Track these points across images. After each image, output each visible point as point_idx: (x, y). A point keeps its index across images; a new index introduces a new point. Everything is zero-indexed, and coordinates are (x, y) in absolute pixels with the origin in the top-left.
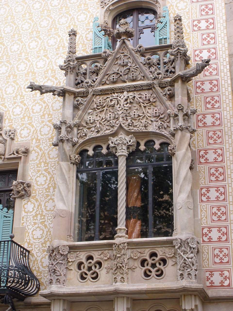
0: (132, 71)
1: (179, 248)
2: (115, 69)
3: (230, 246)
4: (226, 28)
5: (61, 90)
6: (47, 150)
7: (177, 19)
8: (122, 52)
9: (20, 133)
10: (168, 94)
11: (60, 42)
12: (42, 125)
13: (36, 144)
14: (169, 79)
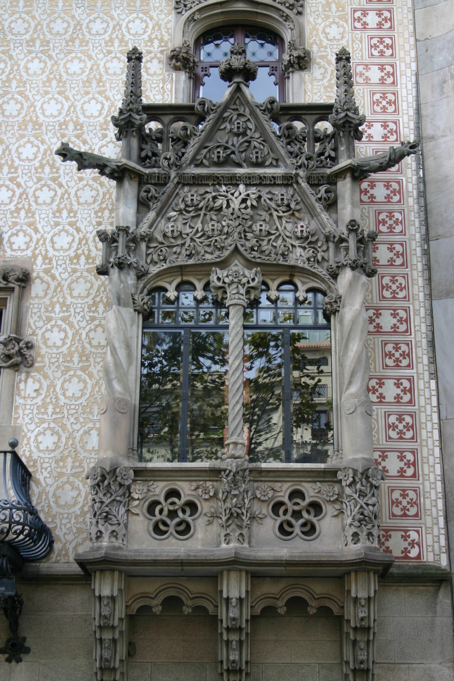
1: (350, 485)
3: (421, 487)
5: (117, 166)
6: (66, 280)
7: (344, 57)
8: (235, 107)
9: (9, 240)
10: (325, 199)
11: (91, 69)
12: (56, 230)
13: (44, 267)
14: (329, 171)
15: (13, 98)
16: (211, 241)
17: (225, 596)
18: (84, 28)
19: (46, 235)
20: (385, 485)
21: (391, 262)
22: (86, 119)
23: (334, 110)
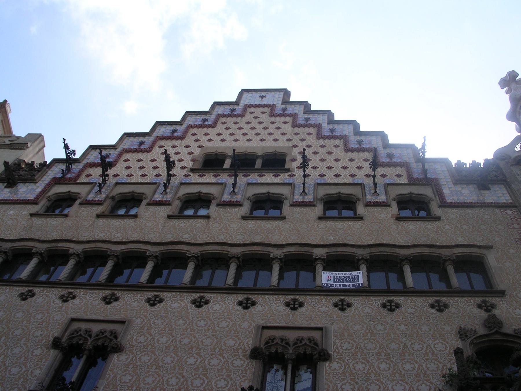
11: (419, 368)
15: (373, 382)
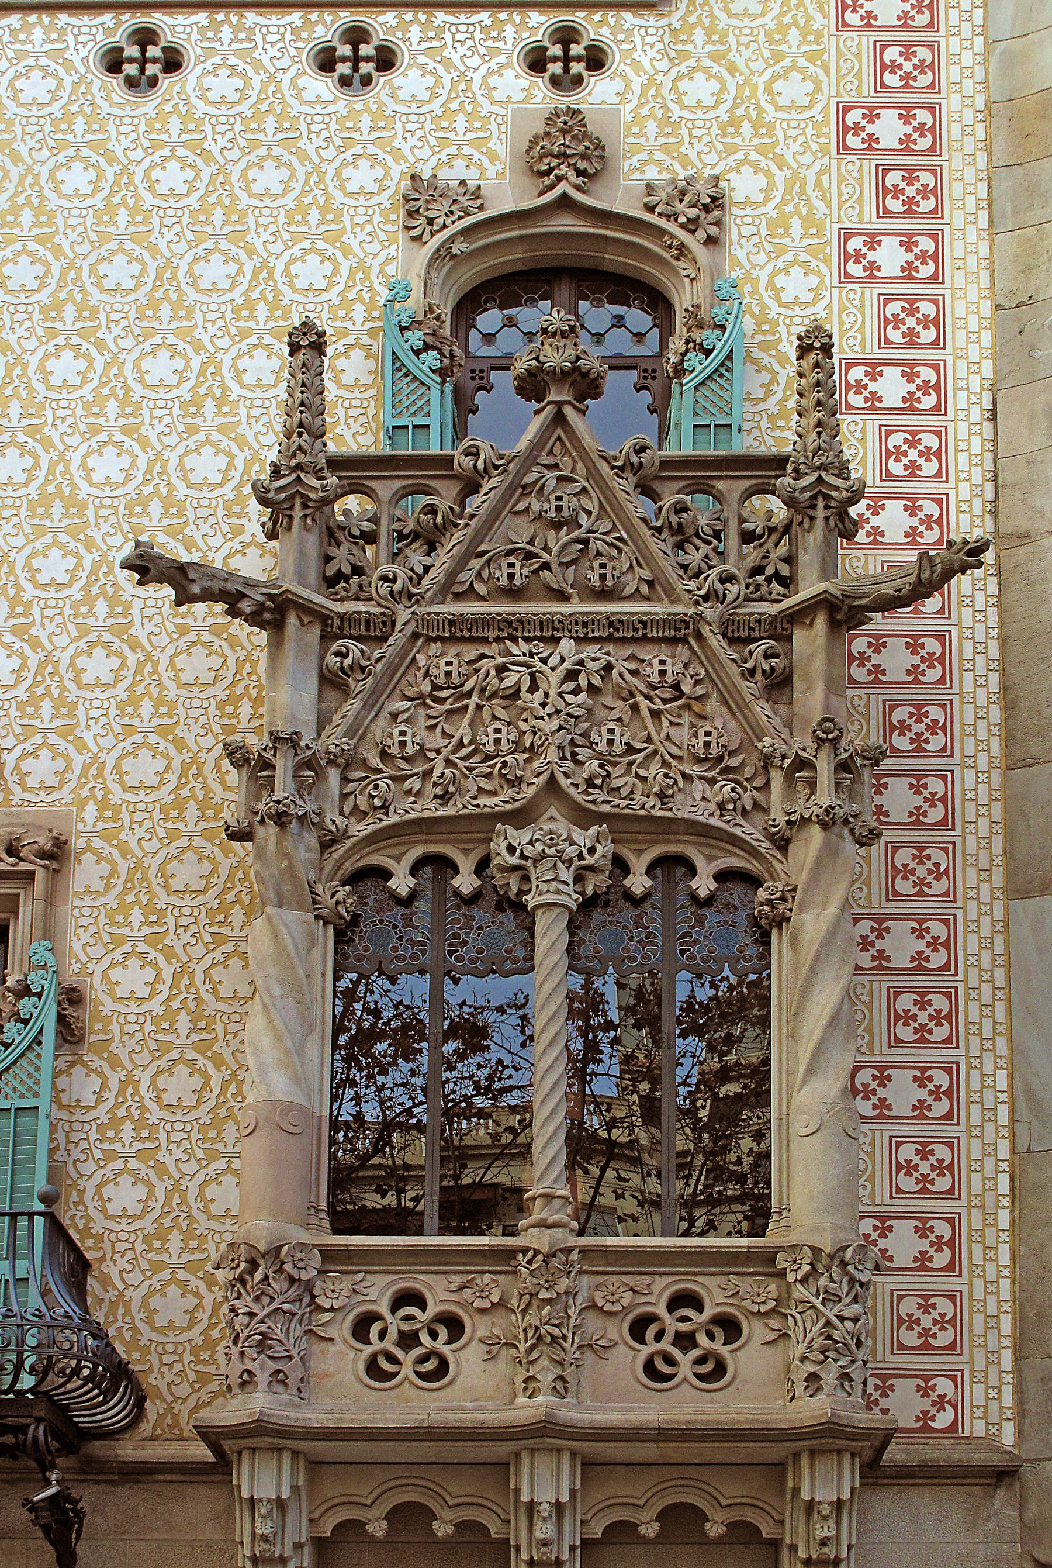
0: (599, 554)
2: (520, 532)
4: (994, 418)
16: (493, 766)
17: (525, 1498)
18: (180, 275)
19: (102, 756)
20: (884, 1285)
21: (917, 818)
22: (192, 492)
23: (789, 468)
